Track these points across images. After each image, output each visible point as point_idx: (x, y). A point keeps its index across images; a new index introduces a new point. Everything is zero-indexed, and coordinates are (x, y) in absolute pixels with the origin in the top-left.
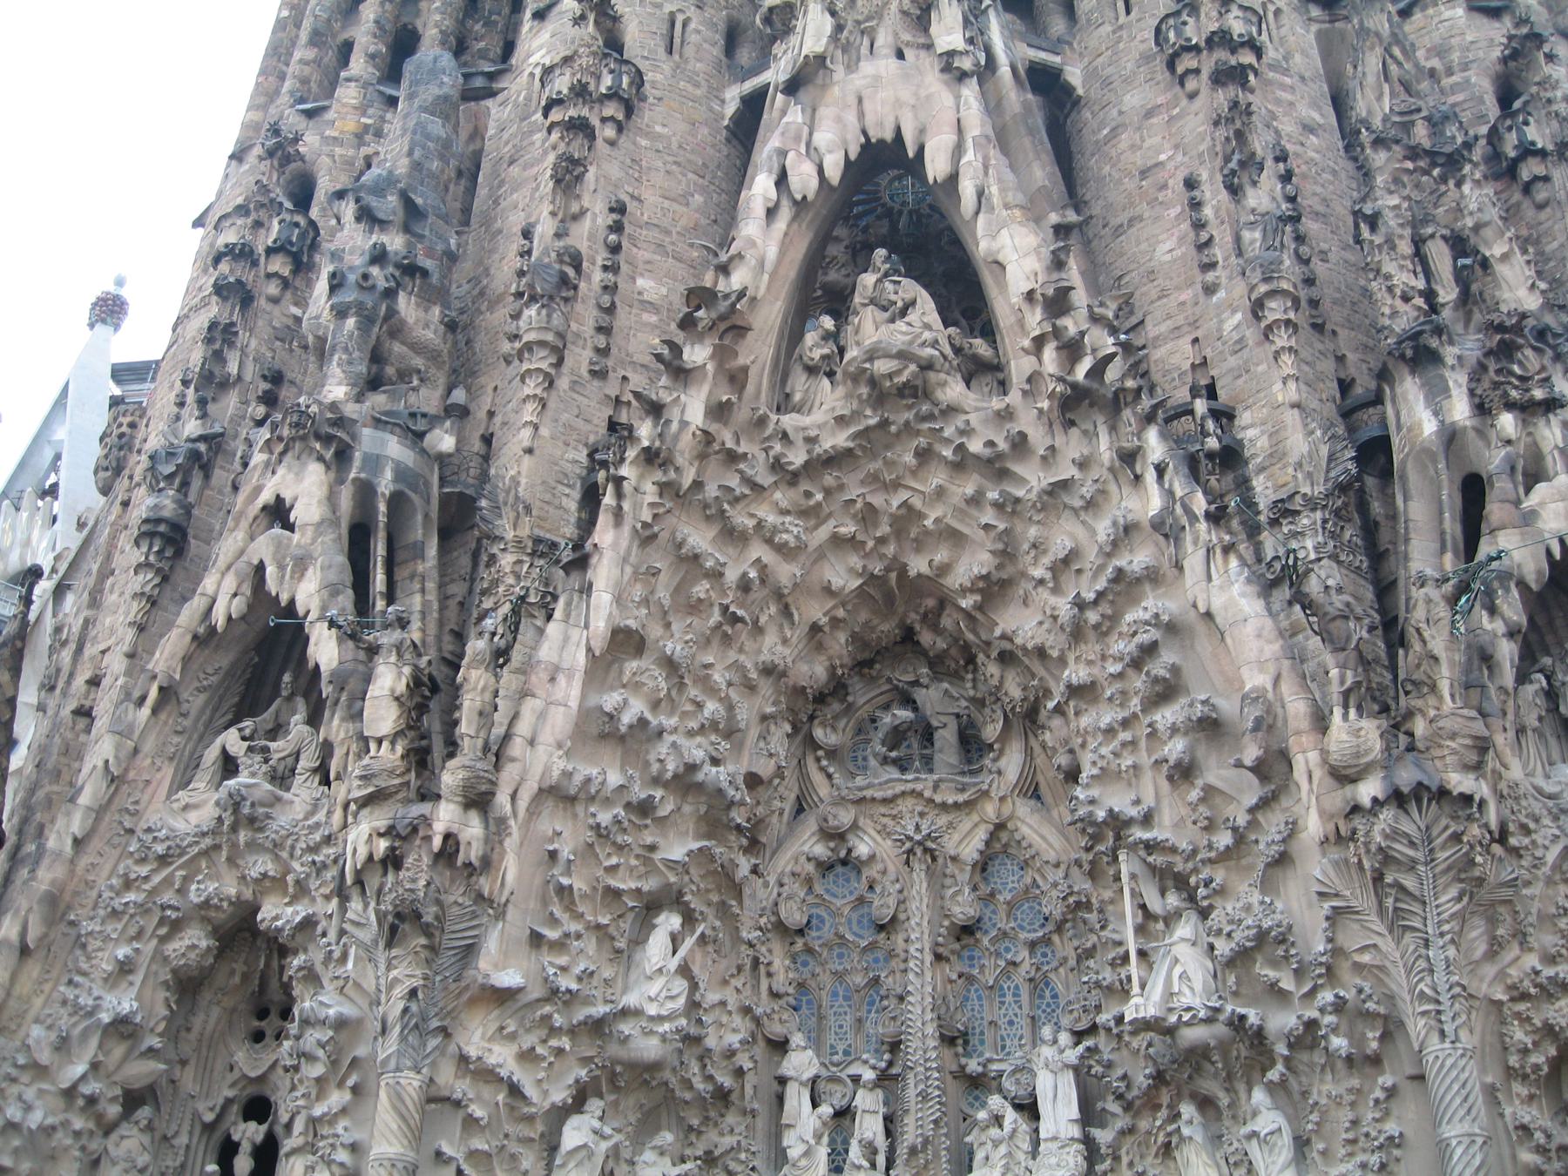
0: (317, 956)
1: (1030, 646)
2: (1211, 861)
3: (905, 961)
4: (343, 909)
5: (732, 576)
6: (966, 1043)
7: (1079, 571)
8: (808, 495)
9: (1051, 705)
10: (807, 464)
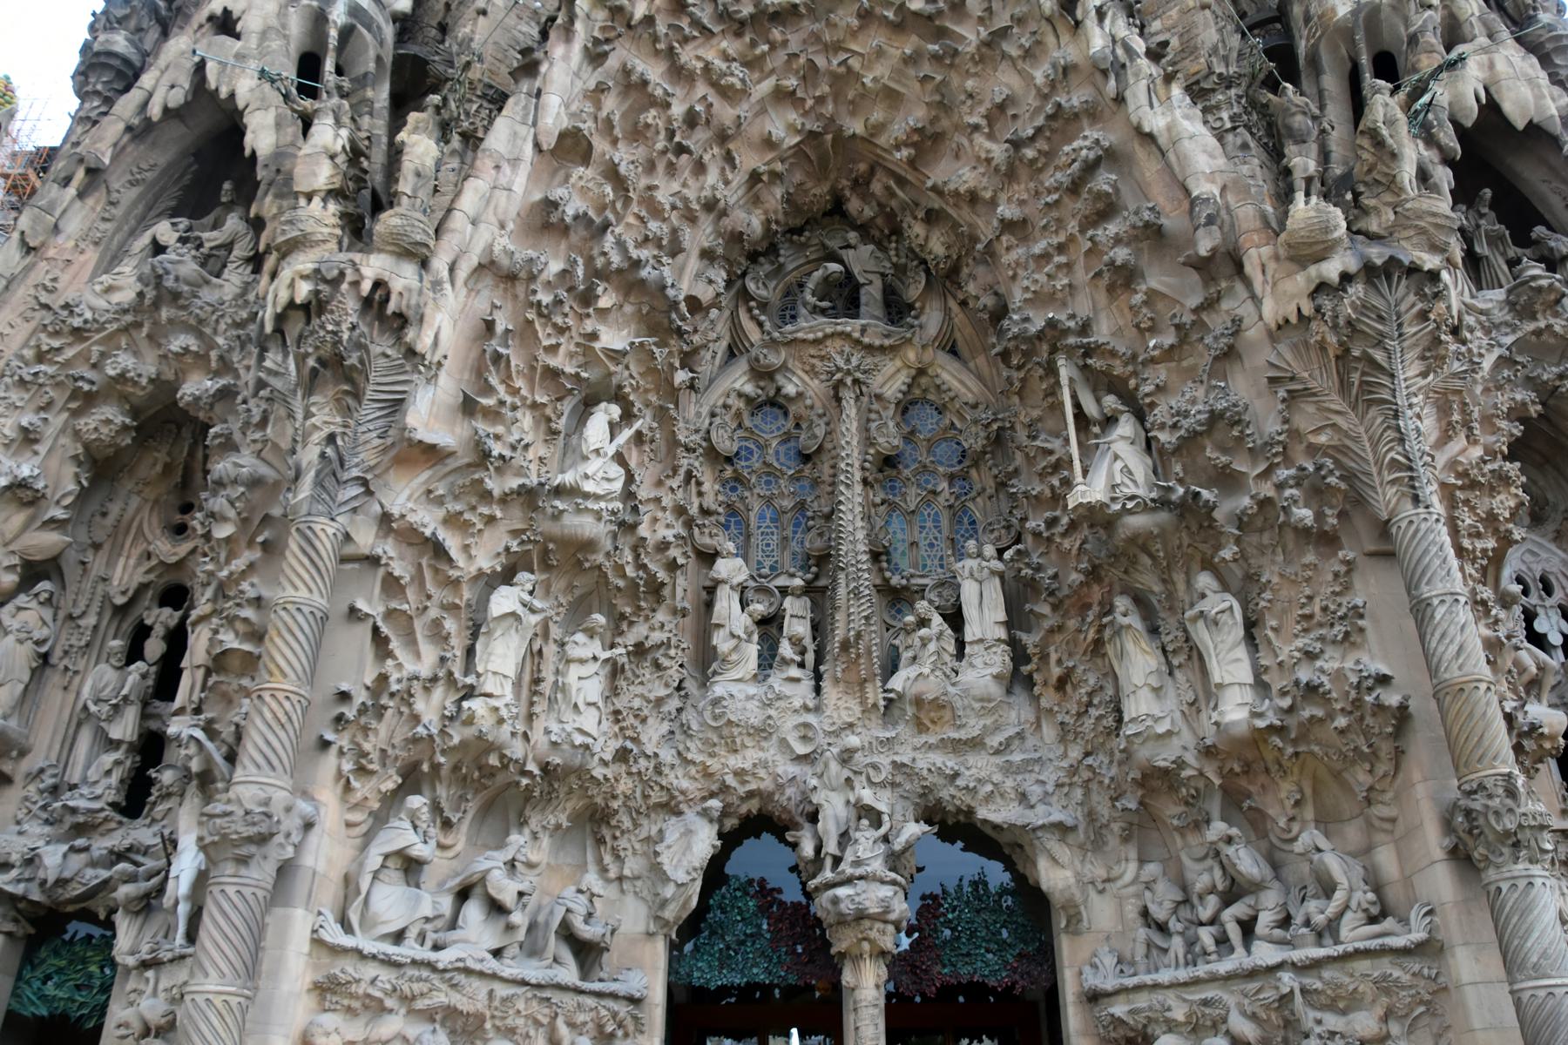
0: (235, 425)
1: (962, 190)
2: (1153, 361)
3: (834, 476)
4: (261, 358)
5: (678, 110)
6: (888, 561)
7: (1015, 117)
8: (753, 44)
9: (979, 247)
10: (752, 16)
